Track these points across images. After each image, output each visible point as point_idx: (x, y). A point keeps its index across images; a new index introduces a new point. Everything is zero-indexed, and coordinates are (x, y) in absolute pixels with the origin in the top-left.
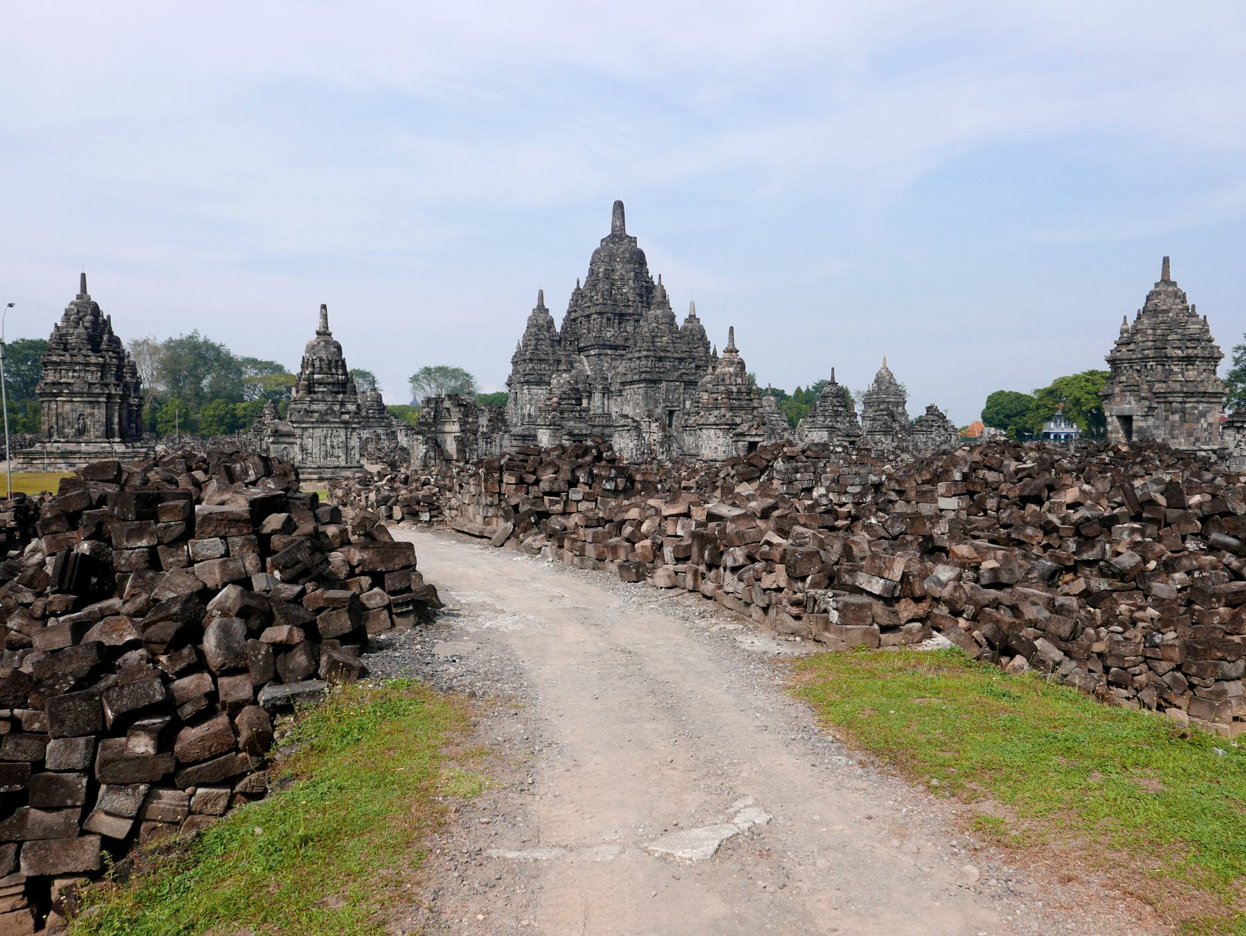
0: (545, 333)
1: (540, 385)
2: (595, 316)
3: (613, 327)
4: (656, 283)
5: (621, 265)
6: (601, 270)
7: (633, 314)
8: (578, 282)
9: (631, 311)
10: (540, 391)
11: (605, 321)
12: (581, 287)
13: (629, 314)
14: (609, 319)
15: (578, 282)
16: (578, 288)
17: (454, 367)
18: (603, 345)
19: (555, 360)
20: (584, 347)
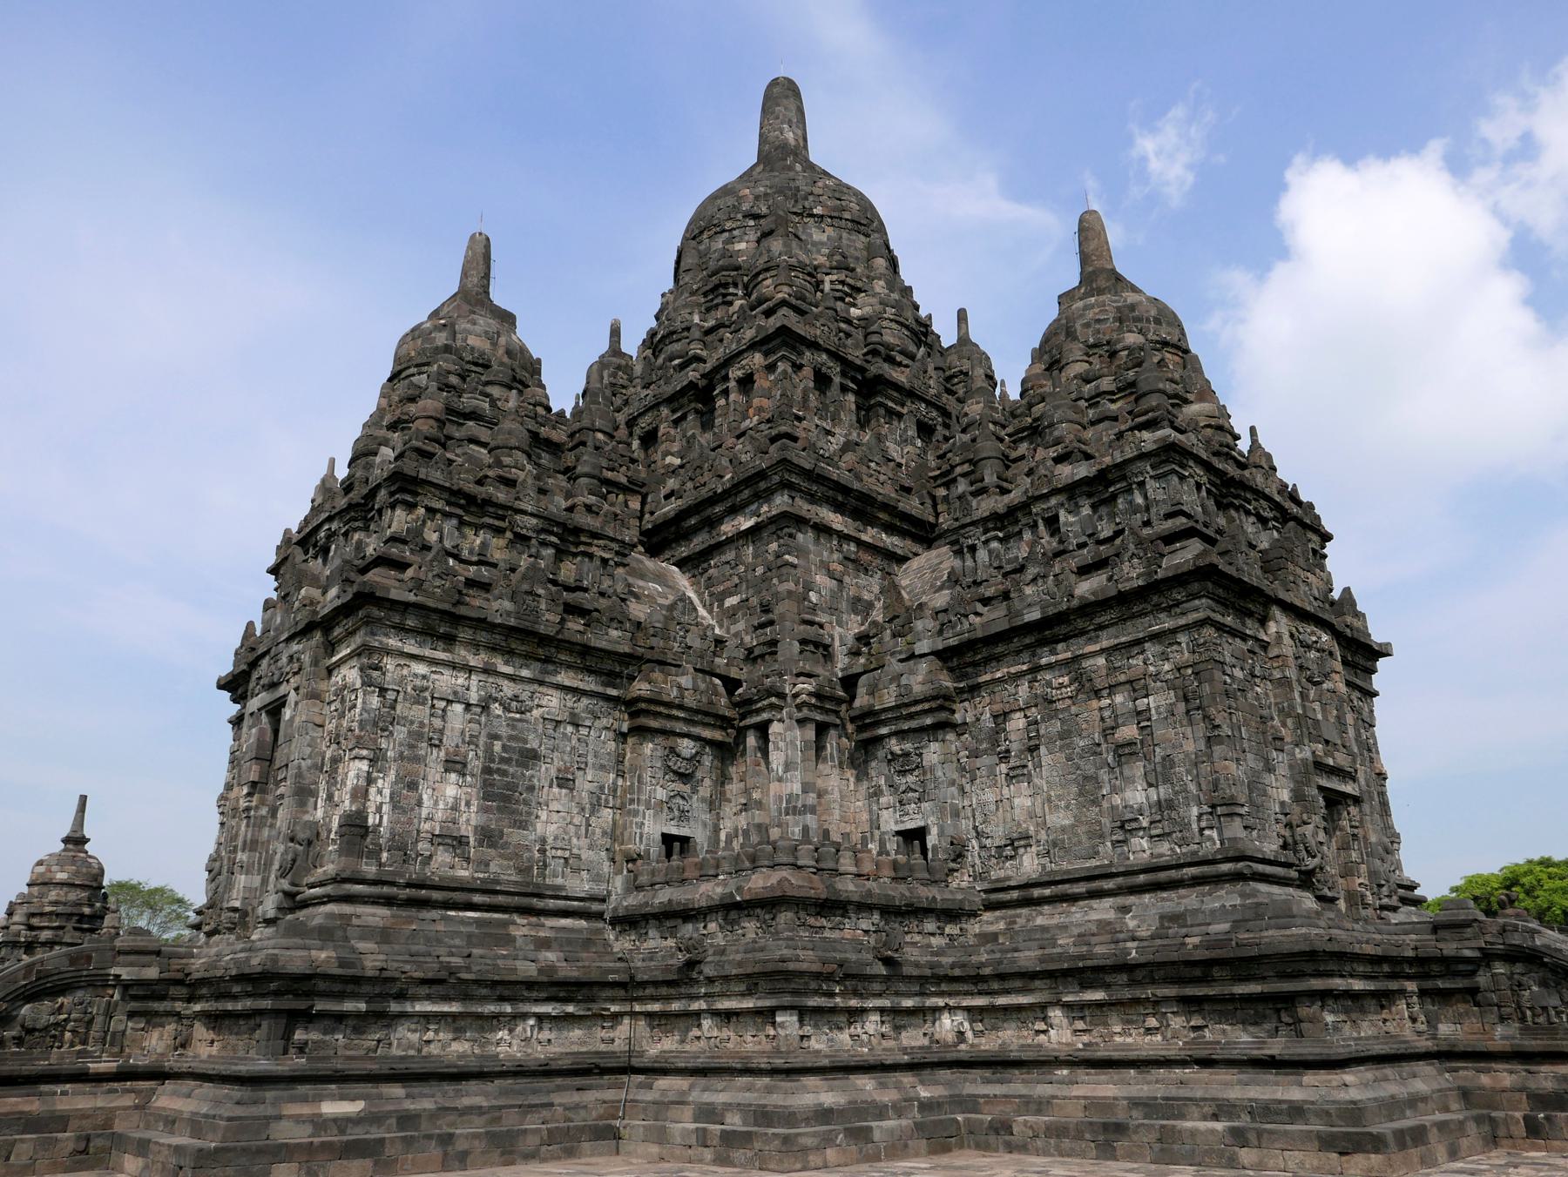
0: (496, 391)
1: (449, 640)
2: (758, 359)
3: (835, 419)
4: (948, 338)
5: (829, 231)
6: (743, 246)
7: (912, 394)
8: (615, 333)
9: (900, 376)
10: (447, 681)
11: (806, 378)
12: (631, 345)
13: (896, 387)
14: (822, 381)
15: (615, 333)
16: (615, 349)
17: (153, 883)
18: (809, 475)
19: (549, 523)
20: (682, 515)
